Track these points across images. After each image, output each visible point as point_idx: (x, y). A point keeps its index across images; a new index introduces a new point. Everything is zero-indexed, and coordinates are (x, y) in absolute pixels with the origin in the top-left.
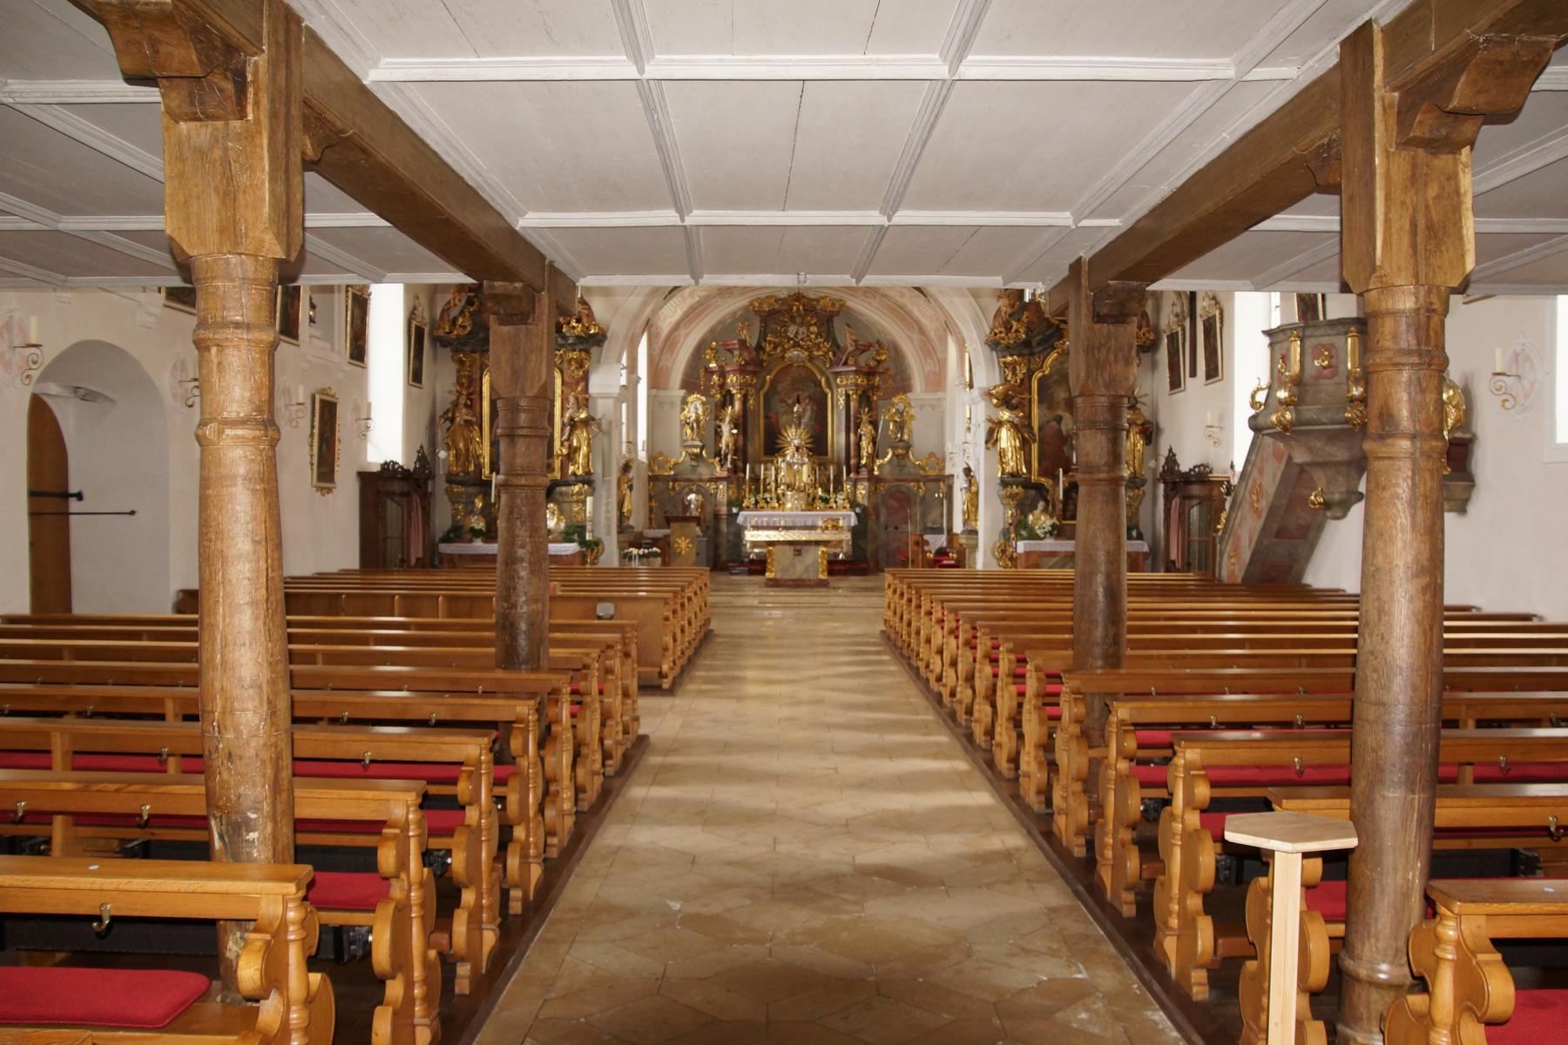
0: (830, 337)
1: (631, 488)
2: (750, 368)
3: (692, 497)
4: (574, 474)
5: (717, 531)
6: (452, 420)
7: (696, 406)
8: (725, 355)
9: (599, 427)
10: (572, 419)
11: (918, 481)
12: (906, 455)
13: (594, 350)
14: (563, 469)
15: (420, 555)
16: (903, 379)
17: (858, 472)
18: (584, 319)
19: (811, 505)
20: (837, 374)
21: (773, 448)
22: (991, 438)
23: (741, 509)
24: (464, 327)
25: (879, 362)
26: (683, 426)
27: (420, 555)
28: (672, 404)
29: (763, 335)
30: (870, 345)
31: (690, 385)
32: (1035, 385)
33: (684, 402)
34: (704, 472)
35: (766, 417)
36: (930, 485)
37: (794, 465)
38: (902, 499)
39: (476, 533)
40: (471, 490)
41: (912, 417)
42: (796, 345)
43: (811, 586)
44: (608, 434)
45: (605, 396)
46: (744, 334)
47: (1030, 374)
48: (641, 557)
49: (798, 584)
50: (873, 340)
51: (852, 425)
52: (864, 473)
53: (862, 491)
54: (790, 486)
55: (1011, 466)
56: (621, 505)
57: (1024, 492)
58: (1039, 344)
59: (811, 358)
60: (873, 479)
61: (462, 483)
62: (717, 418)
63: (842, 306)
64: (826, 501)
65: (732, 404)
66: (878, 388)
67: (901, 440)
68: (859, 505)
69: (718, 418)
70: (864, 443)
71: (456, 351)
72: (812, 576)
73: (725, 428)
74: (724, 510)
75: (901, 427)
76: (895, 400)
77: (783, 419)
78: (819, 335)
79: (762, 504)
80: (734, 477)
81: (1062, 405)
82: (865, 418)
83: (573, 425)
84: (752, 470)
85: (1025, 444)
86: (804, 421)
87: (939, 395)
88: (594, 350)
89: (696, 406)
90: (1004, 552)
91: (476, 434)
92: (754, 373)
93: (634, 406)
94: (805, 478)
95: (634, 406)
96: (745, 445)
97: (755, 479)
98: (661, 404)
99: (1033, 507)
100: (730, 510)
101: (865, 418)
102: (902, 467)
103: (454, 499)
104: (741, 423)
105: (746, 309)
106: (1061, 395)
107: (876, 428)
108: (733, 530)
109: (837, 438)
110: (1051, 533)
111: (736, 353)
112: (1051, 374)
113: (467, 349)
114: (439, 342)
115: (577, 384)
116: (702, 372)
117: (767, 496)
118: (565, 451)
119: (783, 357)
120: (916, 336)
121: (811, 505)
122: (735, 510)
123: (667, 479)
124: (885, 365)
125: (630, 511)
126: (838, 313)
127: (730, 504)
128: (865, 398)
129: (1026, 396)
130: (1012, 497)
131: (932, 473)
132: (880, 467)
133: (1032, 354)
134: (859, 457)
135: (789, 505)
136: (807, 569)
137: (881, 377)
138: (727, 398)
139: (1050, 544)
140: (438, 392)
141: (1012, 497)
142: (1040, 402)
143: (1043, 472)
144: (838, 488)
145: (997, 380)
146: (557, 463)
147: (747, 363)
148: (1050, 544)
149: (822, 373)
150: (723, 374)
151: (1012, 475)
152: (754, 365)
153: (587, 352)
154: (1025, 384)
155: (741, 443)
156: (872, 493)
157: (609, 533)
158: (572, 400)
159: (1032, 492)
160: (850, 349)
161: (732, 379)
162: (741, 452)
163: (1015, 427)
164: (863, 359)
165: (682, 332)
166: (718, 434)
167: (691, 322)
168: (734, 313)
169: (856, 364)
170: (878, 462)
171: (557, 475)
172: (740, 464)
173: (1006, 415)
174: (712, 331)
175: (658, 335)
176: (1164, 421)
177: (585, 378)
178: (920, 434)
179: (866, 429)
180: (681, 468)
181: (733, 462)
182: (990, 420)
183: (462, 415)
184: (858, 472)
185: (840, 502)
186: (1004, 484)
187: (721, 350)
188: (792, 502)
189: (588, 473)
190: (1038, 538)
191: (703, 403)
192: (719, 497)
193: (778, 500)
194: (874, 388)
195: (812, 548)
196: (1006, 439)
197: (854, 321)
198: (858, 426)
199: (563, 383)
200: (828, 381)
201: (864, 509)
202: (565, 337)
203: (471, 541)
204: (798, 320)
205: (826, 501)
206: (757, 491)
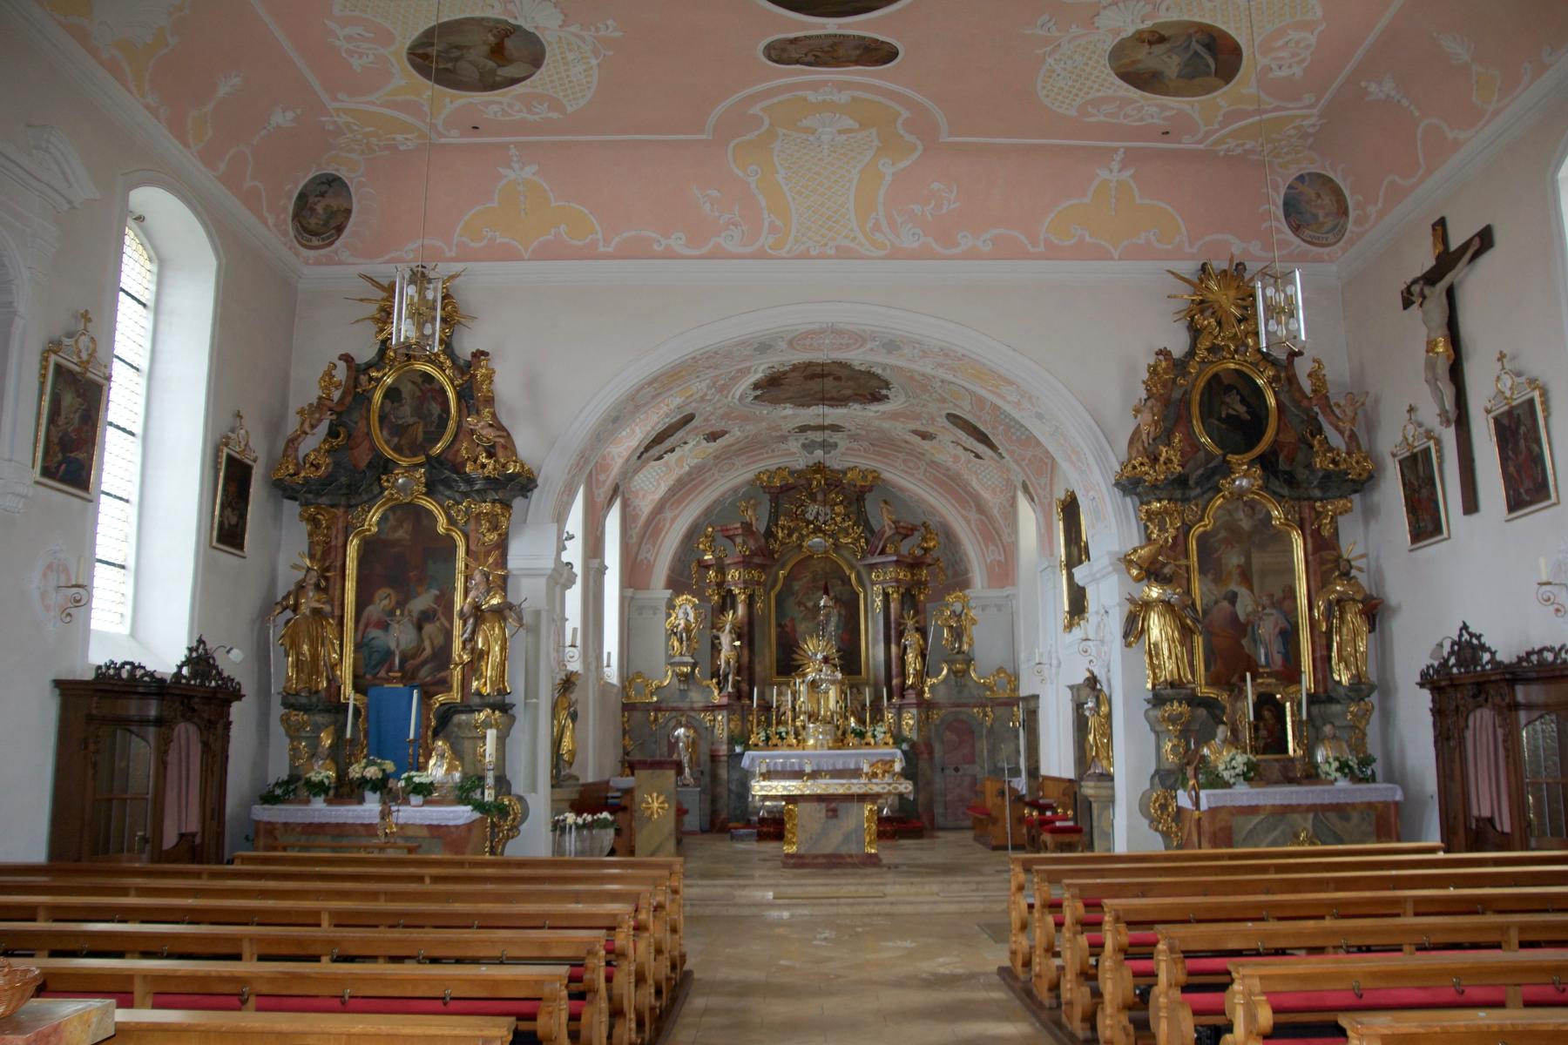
0: (862, 519)
1: (574, 717)
2: (757, 560)
3: (681, 731)
4: (479, 693)
5: (714, 777)
6: (295, 609)
7: (686, 611)
8: (722, 542)
9: (520, 619)
10: (477, 607)
11: (984, 706)
12: (966, 672)
13: (518, 503)
14: (465, 684)
15: (193, 826)
16: (956, 574)
17: (902, 696)
18: (500, 453)
19: (840, 741)
20: (872, 567)
21: (789, 665)
22: (1133, 629)
23: (747, 747)
24: (317, 467)
25: (926, 550)
26: (668, 638)
27: (193, 826)
28: (655, 609)
29: (774, 517)
30: (913, 529)
31: (677, 584)
32: (1193, 545)
33: (671, 606)
34: (697, 698)
35: (779, 625)
36: (1000, 711)
37: (818, 688)
38: (965, 731)
39: (318, 788)
40: (320, 719)
41: (974, 622)
42: (818, 530)
43: (854, 866)
44: (534, 630)
45: (533, 574)
46: (749, 515)
47: (1186, 529)
48: (579, 828)
49: (834, 863)
50: (919, 523)
51: (894, 633)
52: (911, 697)
53: (909, 720)
54: (813, 717)
55: (1169, 668)
56: (557, 743)
57: (1186, 711)
58: (1197, 483)
59: (837, 547)
60: (924, 706)
61: (306, 709)
62: (713, 627)
63: (877, 478)
64: (861, 735)
65: (734, 607)
66: (925, 584)
67: (960, 652)
68: (905, 740)
69: (716, 626)
70: (910, 657)
71: (306, 504)
72: (853, 849)
73: (725, 639)
74: (723, 749)
75: (958, 633)
76: (950, 599)
77: (802, 627)
78: (847, 516)
79: (775, 740)
80: (737, 706)
81: (1236, 577)
82: (910, 623)
83: (478, 614)
84: (761, 696)
85: (1186, 633)
87: (1008, 591)
88: (518, 503)
89: (686, 611)
90: (1161, 812)
91: (330, 633)
92: (762, 567)
93: (581, 594)
94: (832, 704)
95: (581, 594)
96: (751, 661)
97: (766, 708)
98: (641, 609)
99: (1207, 737)
100: (731, 749)
101: (910, 623)
102: (961, 687)
103: (293, 732)
104: (746, 633)
105: (752, 483)
106: (1233, 559)
107: (924, 636)
108: (735, 776)
109: (873, 651)
110: (1246, 777)
111: (739, 540)
112: (1215, 530)
113: (324, 500)
114: (284, 489)
115: (488, 553)
116: (694, 566)
117: (782, 729)
118: (466, 658)
119: (800, 546)
120: (973, 516)
121: (840, 741)
122: (738, 749)
123: (647, 707)
124: (935, 554)
125: (572, 753)
126: (871, 489)
127: (732, 741)
128: (910, 598)
129: (1183, 562)
130: (1172, 720)
131: (1003, 694)
132: (932, 687)
133: (1186, 500)
134: (903, 674)
135: (811, 742)
136: (847, 838)
137: (930, 572)
138: (727, 601)
139: (1243, 794)
140: (283, 568)
141: (1172, 720)
142: (1203, 571)
143: (1213, 681)
144: (877, 717)
145: (1134, 538)
146: (457, 673)
147: (753, 554)
148: (1243, 794)
149: (852, 567)
150: (721, 569)
151: (1172, 685)
152: (762, 558)
153: (507, 505)
154: (1178, 546)
155: (745, 659)
156: (922, 723)
157: (534, 789)
158: (478, 577)
159: (1202, 712)
160: (889, 532)
161: (733, 575)
162: (746, 671)
163: (1167, 606)
164: (905, 548)
165: (668, 514)
166: (715, 648)
167: (679, 502)
168: (735, 490)
169: (896, 552)
170: (929, 681)
171: (456, 695)
172: (745, 687)
173: (1155, 592)
174: (707, 513)
175: (635, 518)
176: (1395, 592)
177: (502, 546)
178: (985, 644)
179: (911, 639)
181: (736, 684)
182: (1131, 600)
183: (310, 601)
184: (902, 696)
185: (880, 736)
186: (1158, 700)
187: (719, 536)
188: (815, 737)
189: (502, 692)
190: (1227, 785)
191: (695, 607)
192: (717, 732)
193: (797, 735)
194: (920, 584)
195: (855, 806)
196: (1157, 628)
197: (891, 497)
198: (901, 635)
199: (467, 553)
200: (859, 577)
201: (913, 745)
202: (469, 481)
203: (308, 802)
204: (820, 497)
205: (861, 735)
206: (769, 725)
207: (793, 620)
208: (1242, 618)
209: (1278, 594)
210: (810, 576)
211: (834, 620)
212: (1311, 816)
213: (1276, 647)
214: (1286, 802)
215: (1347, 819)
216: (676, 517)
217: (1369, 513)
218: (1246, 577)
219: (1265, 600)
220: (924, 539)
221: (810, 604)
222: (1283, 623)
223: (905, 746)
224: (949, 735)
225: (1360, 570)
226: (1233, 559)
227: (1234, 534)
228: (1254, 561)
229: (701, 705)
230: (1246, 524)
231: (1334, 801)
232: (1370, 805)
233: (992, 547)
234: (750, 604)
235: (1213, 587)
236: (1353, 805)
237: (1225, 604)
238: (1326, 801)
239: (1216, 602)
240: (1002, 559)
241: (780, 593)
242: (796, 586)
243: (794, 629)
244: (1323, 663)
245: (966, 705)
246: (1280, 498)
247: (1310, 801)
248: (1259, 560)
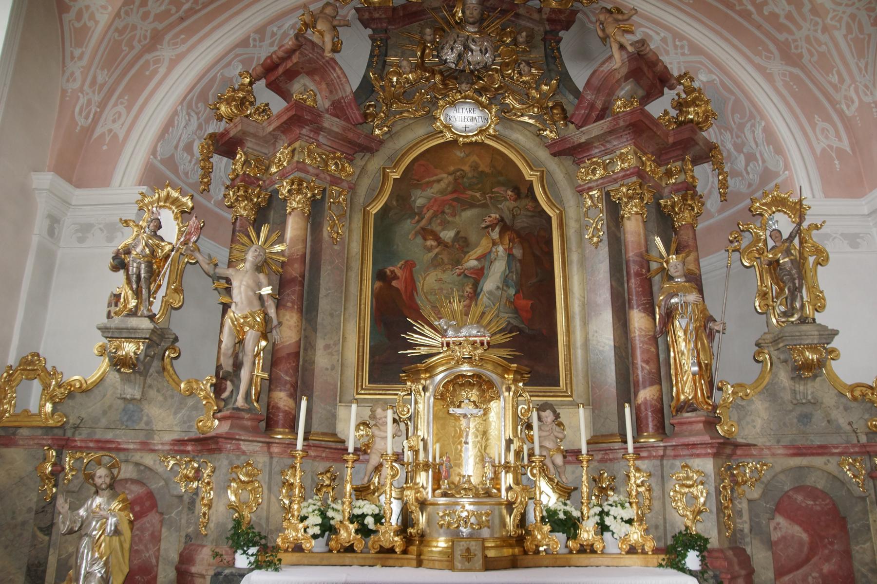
35: (380, 275)
51: (635, 284)
77: (429, 281)
86: (490, 284)
94: (497, 450)
96: (306, 343)
117: (366, 507)
120: (777, 67)
172: (282, 398)
180: (90, 408)
205: (568, 526)
207: (410, 266)
210: (446, 180)
211: (499, 268)
216: (180, 57)
220: (680, 105)
221: (447, 235)
223: (692, 560)
224: (784, 527)
229: (169, 437)
233: (821, 124)
234: (315, 212)
240: (845, 144)
241: (385, 209)
242: (420, 199)
243: (411, 283)
245: (822, 450)
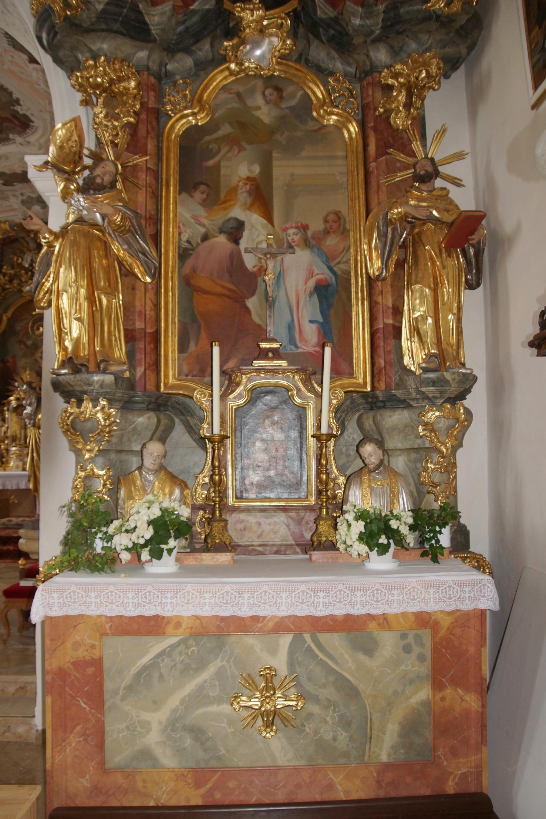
81: (243, 196)
208: (250, 262)
209: (316, 225)
212: (286, 640)
213: (309, 312)
214: (225, 613)
215: (368, 648)
217: (476, 96)
218: (261, 197)
219: (293, 235)
222: (322, 273)
225: (457, 182)
226: (240, 168)
227: (245, 131)
228: (276, 172)
230: (264, 112)
231: (339, 611)
232: (423, 620)
235: (201, 211)
236: (384, 621)
237: (222, 239)
238: (320, 612)
239: (205, 238)
244: (386, 336)
246: (322, 73)
247: (283, 612)
248: (282, 170)
